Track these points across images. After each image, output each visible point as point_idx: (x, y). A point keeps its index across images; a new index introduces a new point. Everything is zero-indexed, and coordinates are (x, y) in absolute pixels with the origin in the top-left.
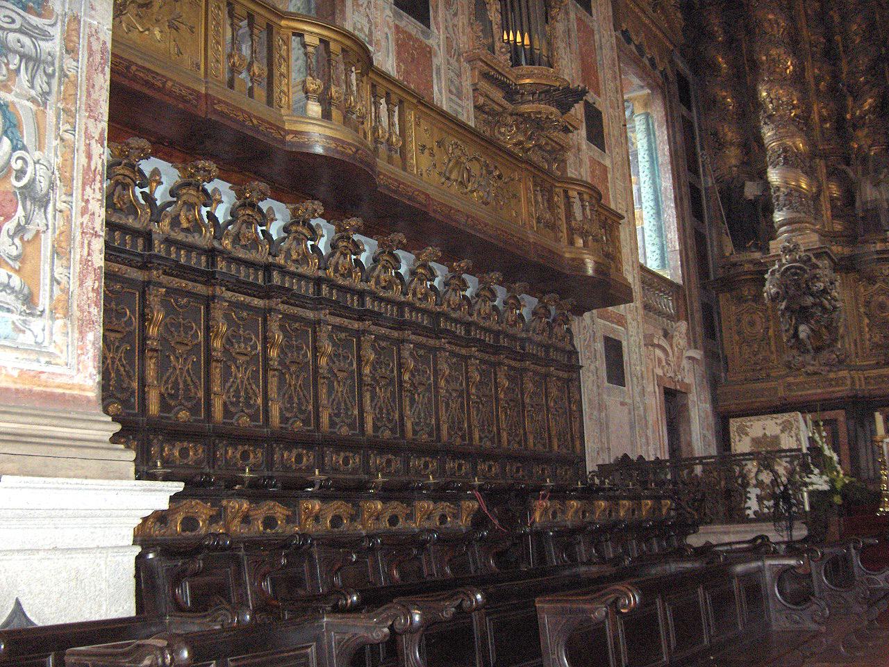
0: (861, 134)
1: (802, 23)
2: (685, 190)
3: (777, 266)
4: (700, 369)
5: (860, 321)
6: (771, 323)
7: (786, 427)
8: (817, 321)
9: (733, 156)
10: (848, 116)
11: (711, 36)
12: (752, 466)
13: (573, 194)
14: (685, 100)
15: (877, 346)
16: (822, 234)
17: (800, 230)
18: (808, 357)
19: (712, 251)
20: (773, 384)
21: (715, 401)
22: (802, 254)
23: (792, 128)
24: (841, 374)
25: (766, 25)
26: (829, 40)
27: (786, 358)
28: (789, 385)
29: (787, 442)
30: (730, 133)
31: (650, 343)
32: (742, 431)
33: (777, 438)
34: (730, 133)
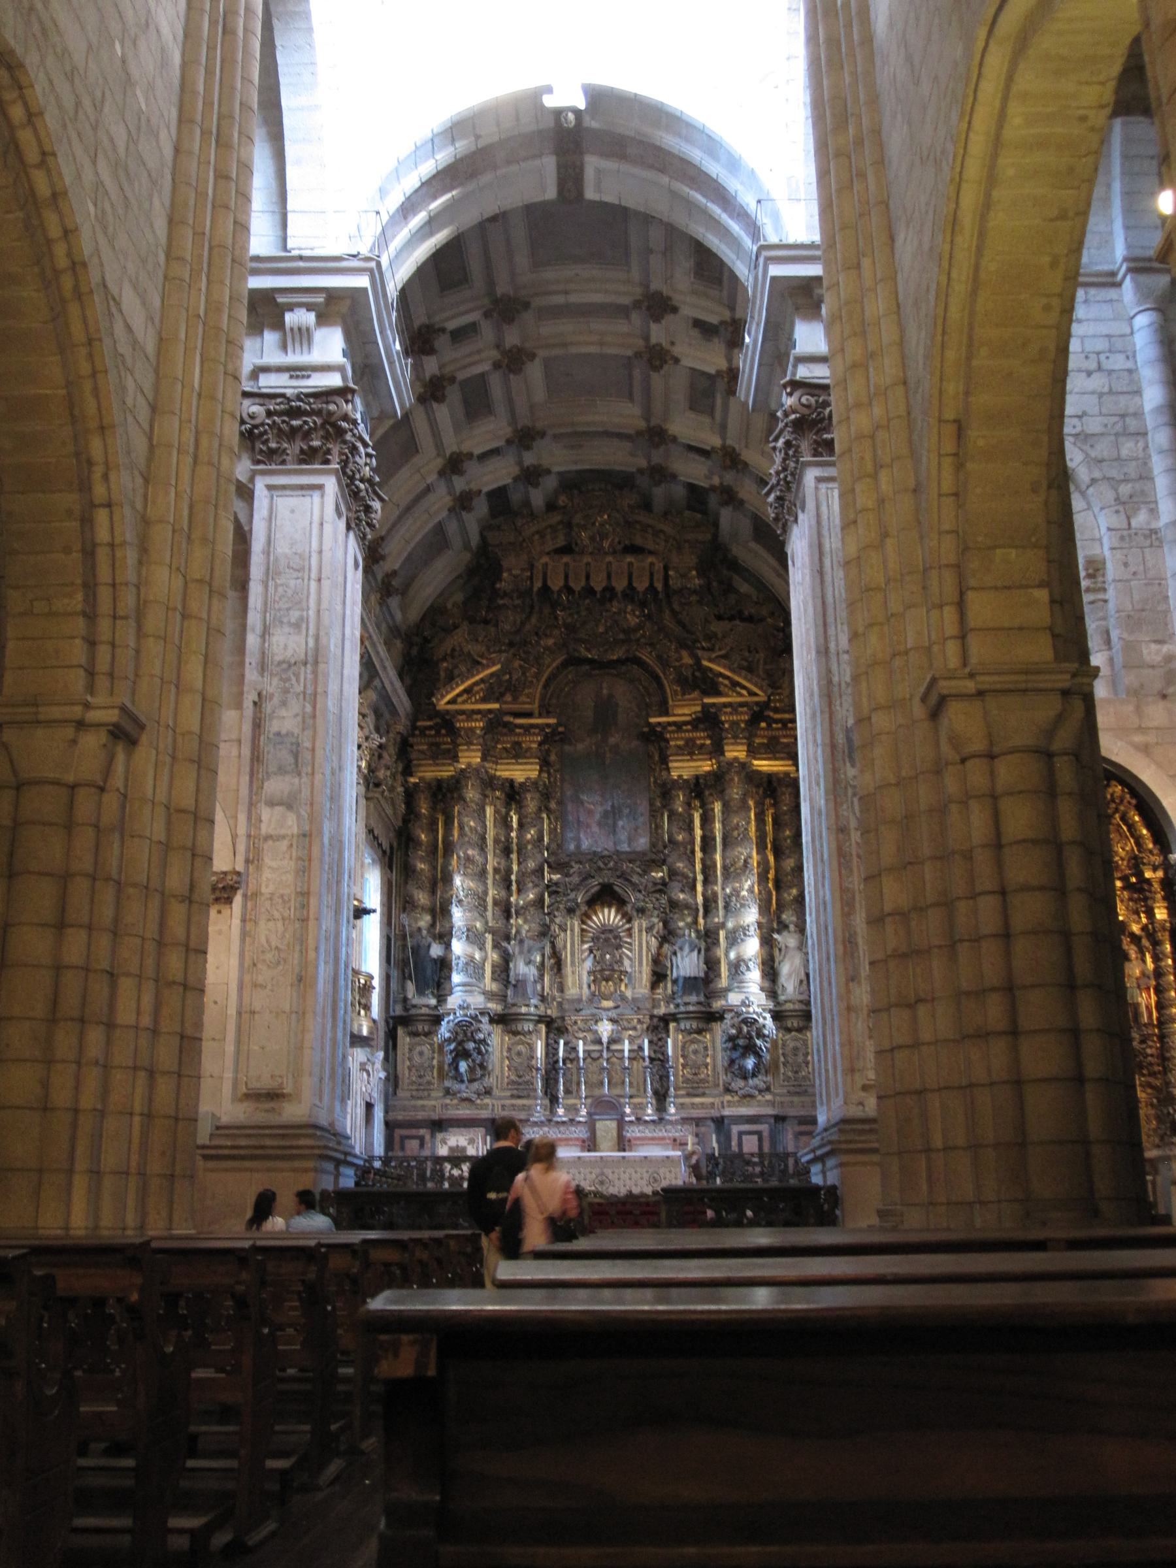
0: (520, 921)
1: (489, 823)
2: (385, 941)
3: (451, 1017)
4: (381, 1085)
5: (502, 1062)
6: (436, 1055)
7: (471, 1141)
8: (473, 1061)
9: (425, 921)
10: (512, 899)
11: (418, 816)
12: (448, 1166)
13: (362, 981)
14: (390, 867)
15: (513, 1083)
16: (484, 993)
17: (471, 992)
18: (463, 1087)
19: (394, 985)
20: (433, 1103)
21: (386, 1112)
22: (471, 1012)
23: (476, 914)
24: (487, 1101)
25: (467, 829)
26: (508, 838)
27: (448, 1083)
28: (446, 1105)
29: (471, 1151)
30: (422, 898)
31: (363, 1067)
32: (444, 1142)
33: (464, 1149)
34: (422, 898)
